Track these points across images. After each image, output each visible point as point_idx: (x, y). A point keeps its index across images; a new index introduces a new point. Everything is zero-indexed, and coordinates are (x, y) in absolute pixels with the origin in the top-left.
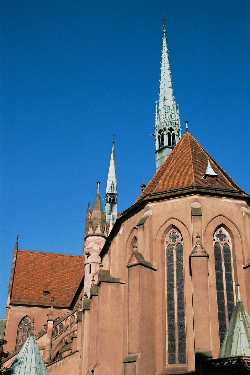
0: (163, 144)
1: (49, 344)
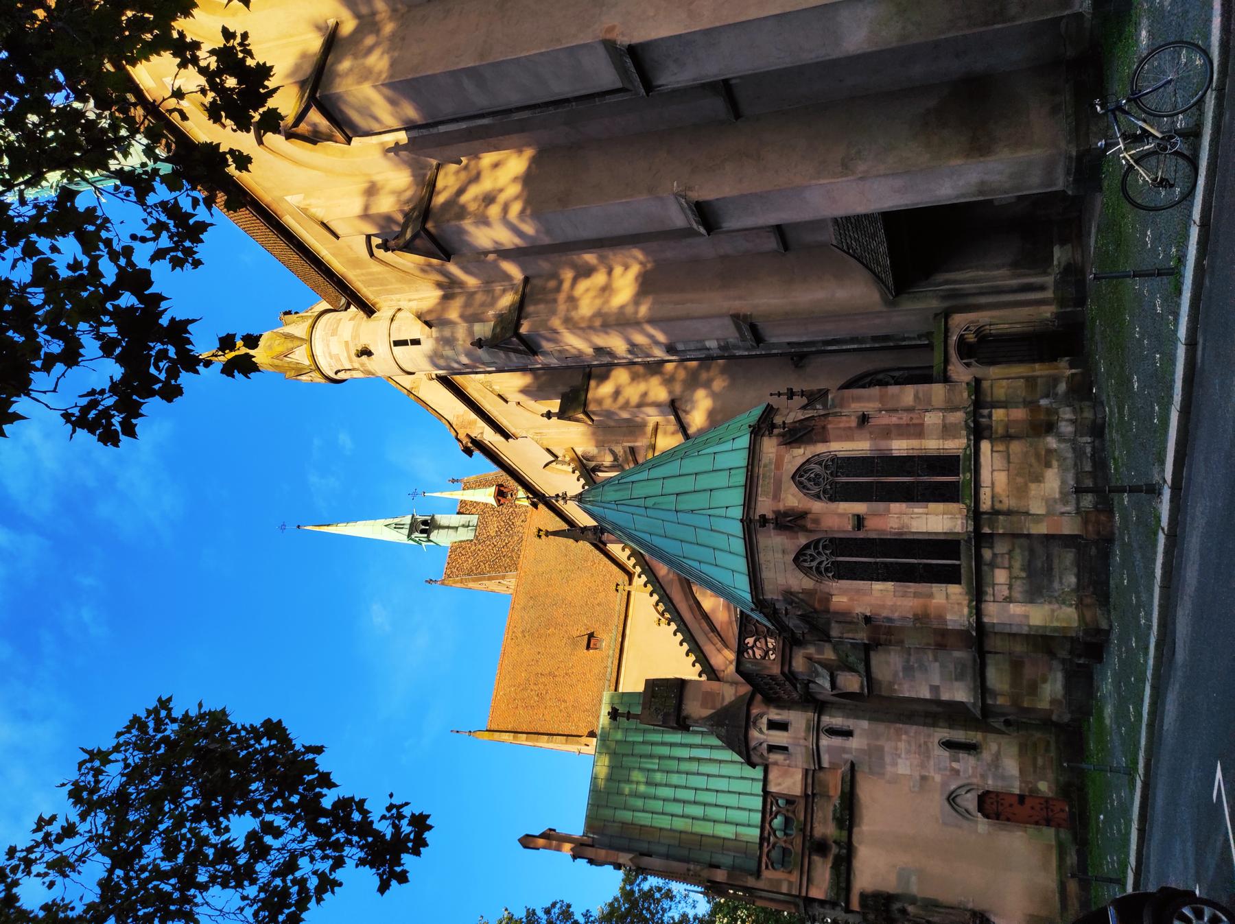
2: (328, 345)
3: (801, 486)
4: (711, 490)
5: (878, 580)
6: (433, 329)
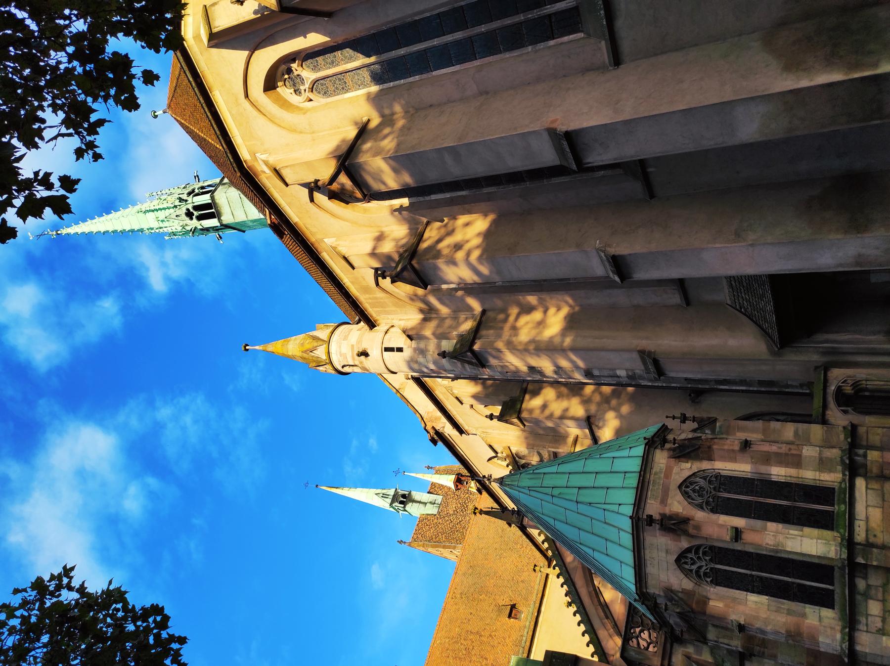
2: (340, 347)
3: (686, 495)
4: (608, 488)
5: (753, 592)
6: (413, 341)
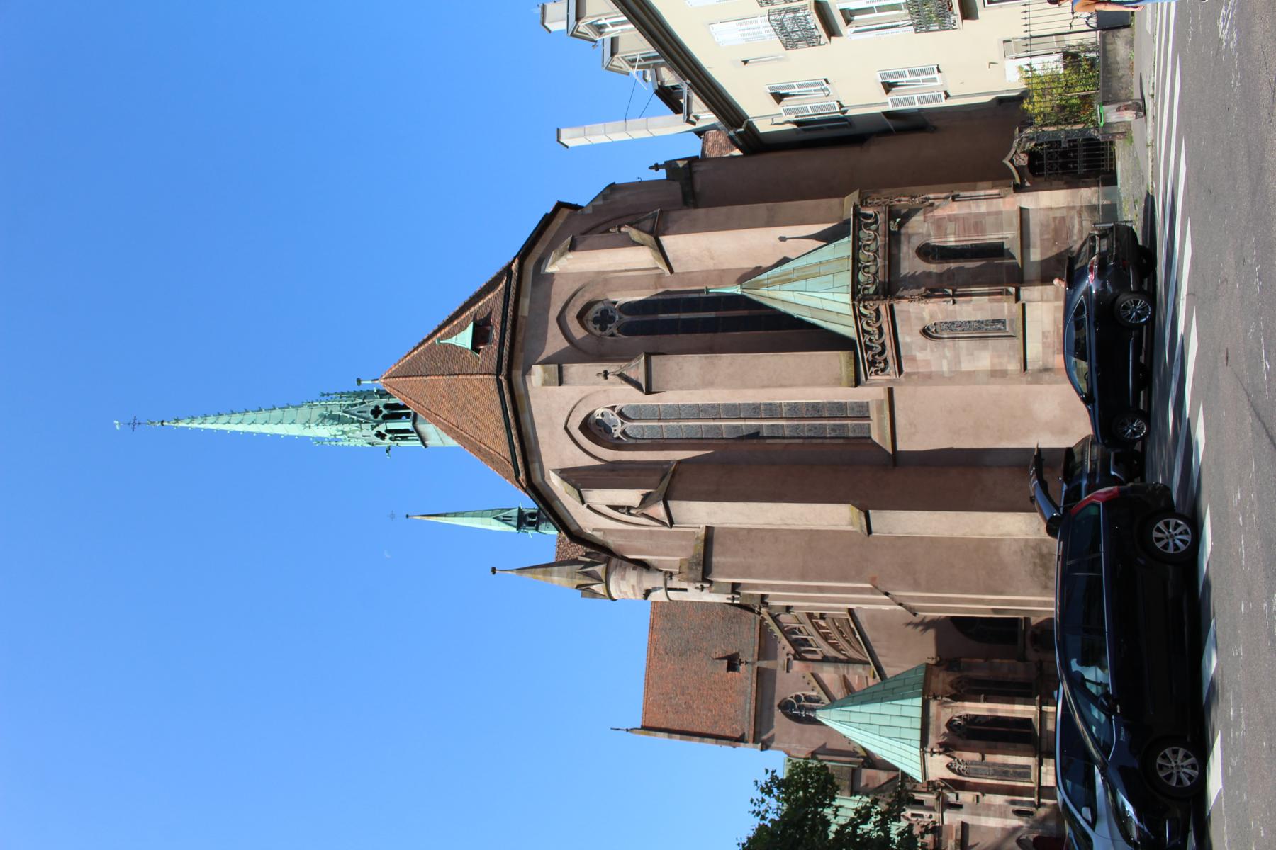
0: (406, 431)
1: (835, 668)
2: (619, 586)
